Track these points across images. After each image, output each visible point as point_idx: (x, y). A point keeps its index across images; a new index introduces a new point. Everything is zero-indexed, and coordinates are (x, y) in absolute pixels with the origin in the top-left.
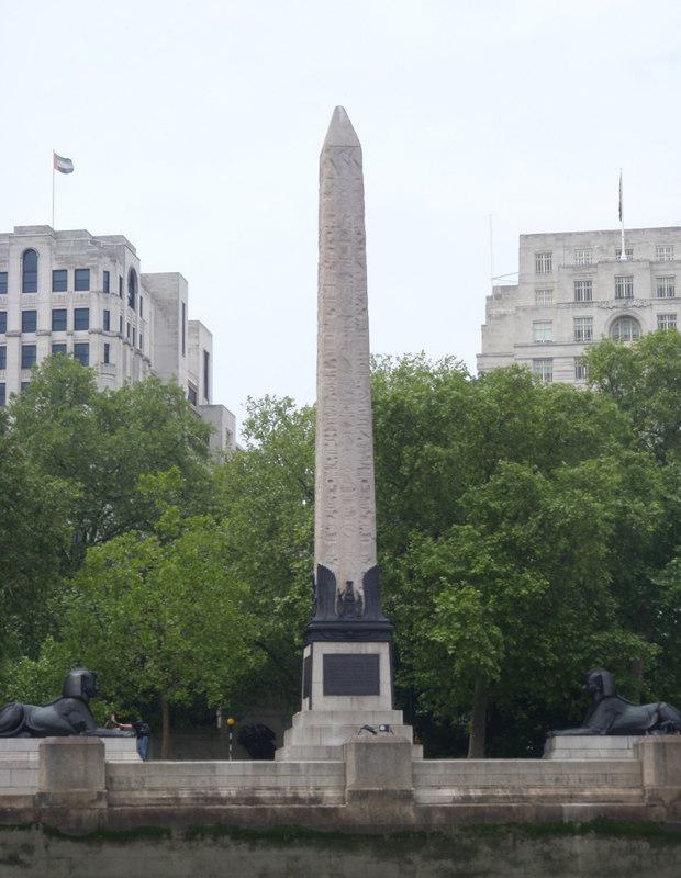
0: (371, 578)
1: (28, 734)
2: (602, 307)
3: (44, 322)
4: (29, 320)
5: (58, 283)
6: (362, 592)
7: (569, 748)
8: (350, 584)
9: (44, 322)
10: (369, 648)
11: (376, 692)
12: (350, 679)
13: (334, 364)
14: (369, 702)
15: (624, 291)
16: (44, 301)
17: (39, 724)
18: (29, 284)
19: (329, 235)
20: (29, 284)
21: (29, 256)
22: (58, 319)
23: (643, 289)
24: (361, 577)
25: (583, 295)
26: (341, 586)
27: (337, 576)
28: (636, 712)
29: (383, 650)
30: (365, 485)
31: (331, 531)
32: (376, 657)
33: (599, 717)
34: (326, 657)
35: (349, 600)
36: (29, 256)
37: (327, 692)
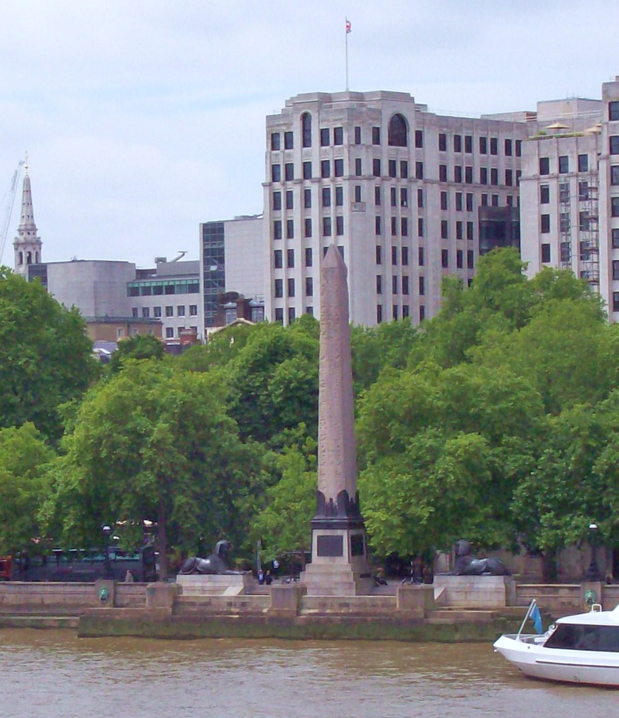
1: (197, 573)
6: (336, 504)
8: (331, 499)
10: (339, 532)
11: (340, 554)
12: (330, 548)
13: (325, 385)
14: (338, 559)
17: (202, 568)
19: (323, 317)
24: (336, 496)
26: (327, 500)
27: (325, 496)
30: (338, 448)
31: (323, 473)
32: (342, 537)
34: (319, 537)
37: (318, 555)
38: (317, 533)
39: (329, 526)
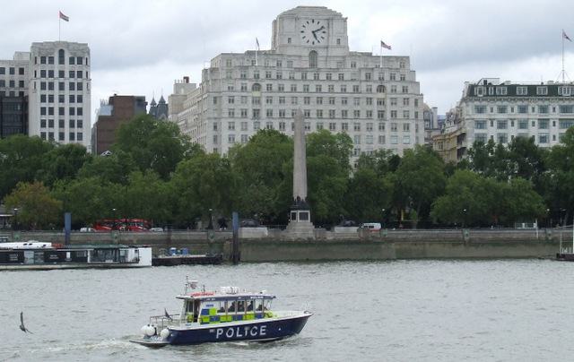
0: (306, 198)
2: (250, 80)
3: (67, 75)
4: (62, 74)
5: (72, 61)
7: (339, 230)
9: (67, 75)
12: (303, 217)
15: (257, 77)
16: (67, 67)
18: (62, 61)
20: (62, 61)
21: (62, 52)
22: (72, 74)
23: (262, 75)
25: (244, 77)
28: (348, 222)
29: (308, 212)
33: (342, 223)
35: (303, 202)
36: (62, 52)
38: (299, 211)
39: (304, 209)
